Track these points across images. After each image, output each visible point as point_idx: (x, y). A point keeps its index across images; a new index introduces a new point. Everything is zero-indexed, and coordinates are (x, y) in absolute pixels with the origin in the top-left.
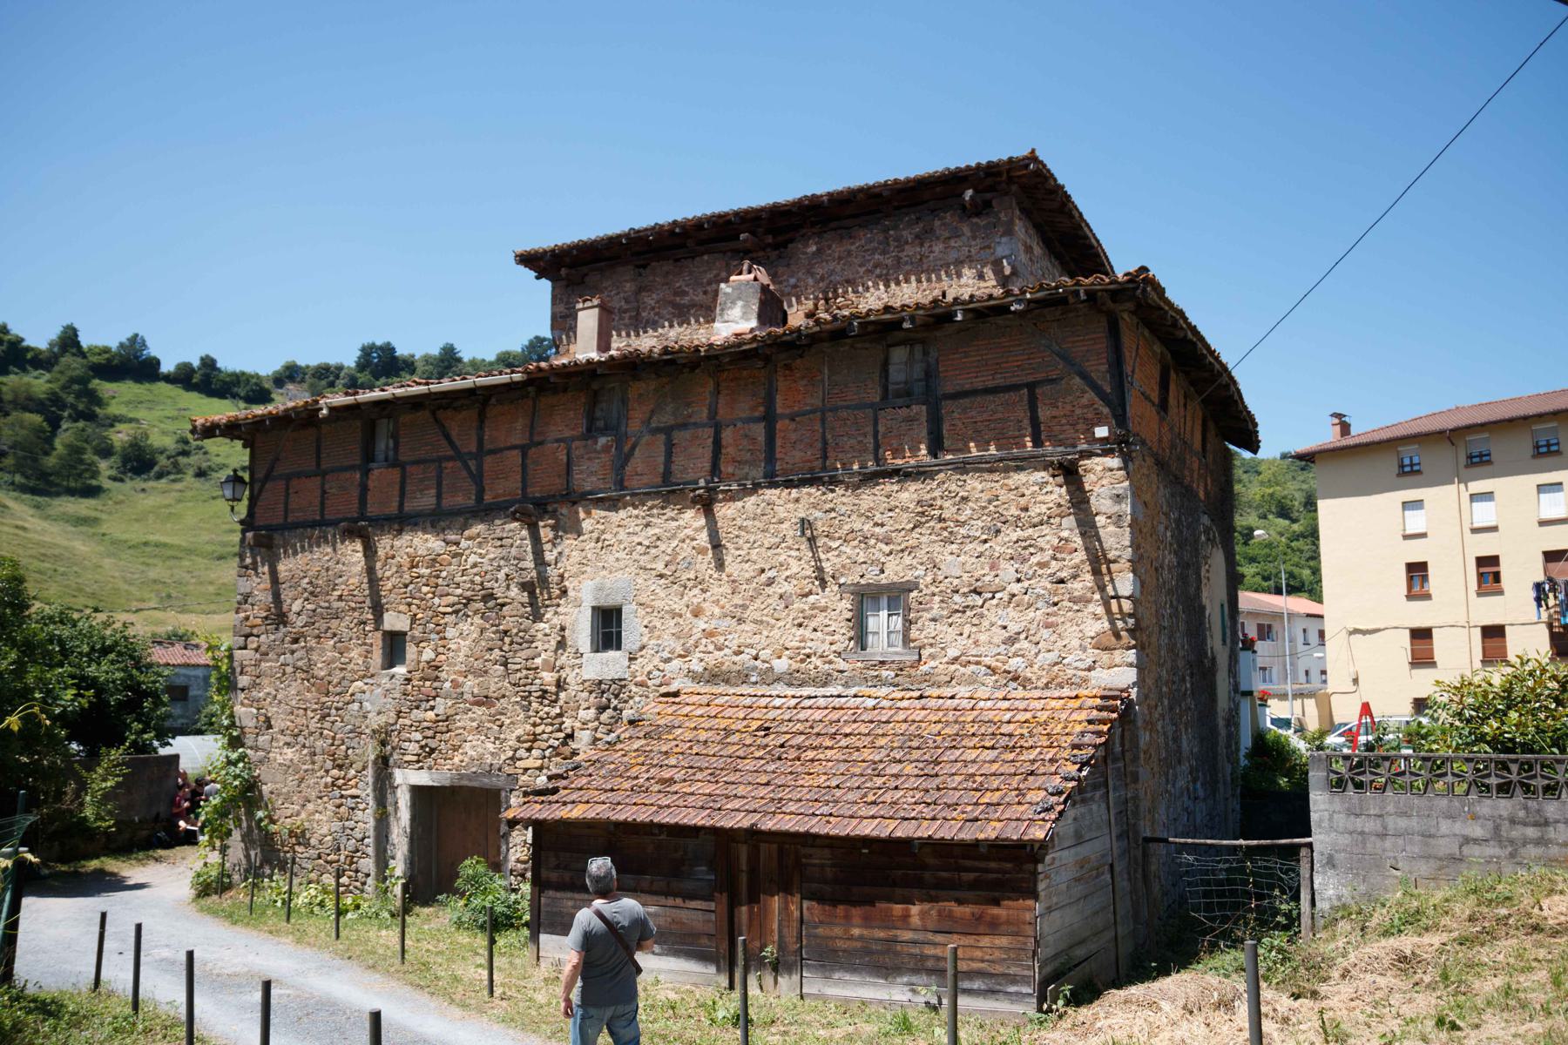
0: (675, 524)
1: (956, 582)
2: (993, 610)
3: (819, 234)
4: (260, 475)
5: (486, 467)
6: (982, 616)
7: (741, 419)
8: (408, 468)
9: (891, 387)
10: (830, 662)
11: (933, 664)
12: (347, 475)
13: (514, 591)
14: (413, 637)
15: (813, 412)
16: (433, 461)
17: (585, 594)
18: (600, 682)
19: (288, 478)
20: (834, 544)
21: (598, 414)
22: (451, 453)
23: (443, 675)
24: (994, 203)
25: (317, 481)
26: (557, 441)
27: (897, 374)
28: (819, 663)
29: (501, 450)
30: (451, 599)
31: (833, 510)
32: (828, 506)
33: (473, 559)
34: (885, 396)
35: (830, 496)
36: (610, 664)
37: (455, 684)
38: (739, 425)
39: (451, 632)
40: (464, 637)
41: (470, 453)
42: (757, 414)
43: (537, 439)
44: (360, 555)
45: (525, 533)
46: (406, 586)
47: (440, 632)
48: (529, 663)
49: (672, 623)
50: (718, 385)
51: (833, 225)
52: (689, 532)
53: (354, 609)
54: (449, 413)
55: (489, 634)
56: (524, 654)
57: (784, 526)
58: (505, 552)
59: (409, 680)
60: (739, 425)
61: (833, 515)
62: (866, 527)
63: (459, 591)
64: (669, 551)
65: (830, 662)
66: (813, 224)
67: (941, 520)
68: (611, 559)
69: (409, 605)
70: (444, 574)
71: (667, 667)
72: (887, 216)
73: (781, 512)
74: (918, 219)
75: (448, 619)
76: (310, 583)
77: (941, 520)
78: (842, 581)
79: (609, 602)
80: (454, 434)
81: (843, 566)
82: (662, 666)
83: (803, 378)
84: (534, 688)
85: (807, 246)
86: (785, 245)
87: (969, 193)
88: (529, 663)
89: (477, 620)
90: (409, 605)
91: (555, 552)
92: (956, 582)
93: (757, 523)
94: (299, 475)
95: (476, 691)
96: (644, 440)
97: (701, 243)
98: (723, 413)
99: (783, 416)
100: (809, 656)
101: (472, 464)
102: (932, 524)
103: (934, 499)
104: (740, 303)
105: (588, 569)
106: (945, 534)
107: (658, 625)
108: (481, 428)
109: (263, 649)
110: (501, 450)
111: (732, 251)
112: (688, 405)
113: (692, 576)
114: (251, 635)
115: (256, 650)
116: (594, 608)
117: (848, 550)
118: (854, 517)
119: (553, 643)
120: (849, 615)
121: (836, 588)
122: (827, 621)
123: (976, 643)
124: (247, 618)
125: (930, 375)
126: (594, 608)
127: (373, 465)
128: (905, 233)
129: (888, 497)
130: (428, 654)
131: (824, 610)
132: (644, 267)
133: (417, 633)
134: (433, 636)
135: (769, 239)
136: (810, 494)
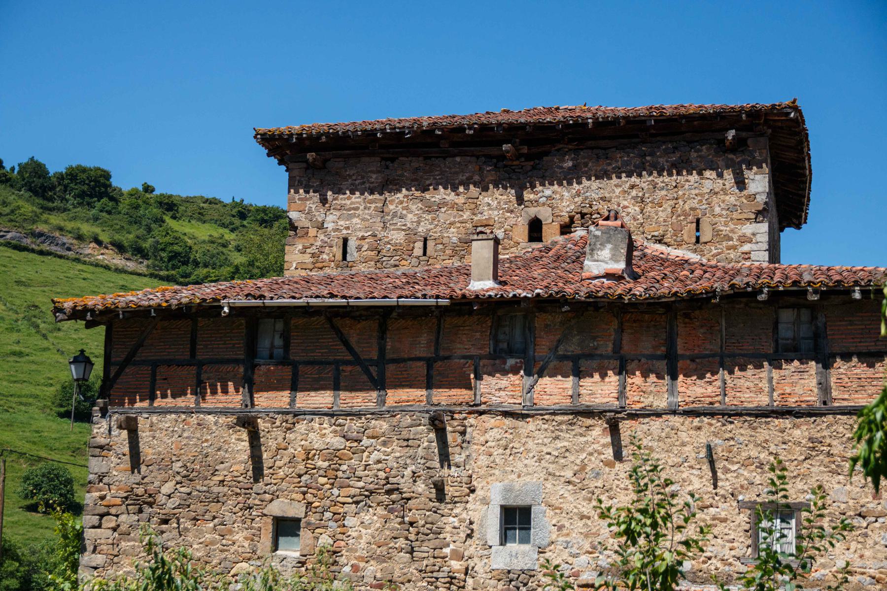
0: (583, 439)
1: (843, 506)
2: (877, 531)
3: (576, 151)
4: (119, 356)
5: (388, 374)
6: (866, 535)
7: (644, 356)
8: (301, 368)
9: (780, 341)
10: (730, 564)
11: (823, 572)
12: (230, 367)
13: (421, 487)
14: (309, 524)
15: (713, 356)
16: (329, 363)
17: (493, 494)
18: (509, 572)
19: (155, 365)
20: (735, 467)
21: (501, 337)
22: (350, 358)
23: (343, 560)
24: (749, 142)
25: (193, 370)
26: (464, 357)
27: (786, 332)
28: (719, 565)
29: (404, 360)
30: (353, 491)
31: (732, 438)
32: (728, 435)
33: (375, 456)
34: (776, 351)
35: (730, 427)
36: (517, 555)
37: (355, 568)
38: (643, 360)
39: (350, 521)
40: (365, 527)
41: (371, 360)
42: (659, 353)
43: (442, 353)
44: (247, 444)
45: (432, 435)
46: (300, 476)
47: (339, 518)
48: (437, 553)
49: (581, 524)
50: (621, 324)
51: (589, 143)
52: (596, 446)
53: (237, 494)
54: (348, 321)
55: (395, 523)
56: (432, 544)
57: (686, 449)
58: (411, 451)
59: (303, 564)
60: (643, 360)
61: (732, 443)
62: (762, 456)
63: (361, 484)
64: (578, 462)
65: (730, 564)
66: (570, 141)
67: (829, 454)
68: (520, 465)
69: (304, 493)
70: (344, 467)
71: (574, 561)
72: (644, 142)
73: (684, 436)
74: (675, 148)
75: (346, 508)
76: (185, 466)
77: (829, 454)
78: (740, 498)
79: (520, 502)
80: (353, 341)
81: (742, 487)
82: (570, 560)
83: (702, 327)
84: (441, 575)
85: (563, 161)
86: (540, 156)
87: (731, 134)
88: (437, 553)
89: (381, 511)
90: (304, 493)
91: (463, 456)
92: (843, 506)
93: (661, 444)
94: (169, 363)
95: (379, 575)
96: (551, 365)
97: (454, 144)
98: (627, 348)
99: (683, 356)
100: (710, 558)
101: (373, 370)
102: (821, 457)
103: (824, 437)
104: (609, 246)
105: (497, 472)
106: (833, 466)
107: (567, 524)
108: (382, 337)
109: (123, 528)
110: (404, 360)
111: (485, 156)
112: (594, 338)
113: (600, 484)
114: (108, 514)
115: (114, 530)
116: (502, 507)
117: (745, 473)
118: (751, 446)
119: (463, 535)
120: (747, 527)
121: (735, 504)
122: (726, 531)
123: (861, 556)
124: (102, 498)
125: (817, 336)
126: (502, 507)
127: (257, 361)
128: (661, 160)
129: (783, 431)
130: (325, 540)
131: (724, 520)
132: (393, 160)
133: (313, 519)
134: (331, 523)
135: (525, 150)
136: (711, 425)
